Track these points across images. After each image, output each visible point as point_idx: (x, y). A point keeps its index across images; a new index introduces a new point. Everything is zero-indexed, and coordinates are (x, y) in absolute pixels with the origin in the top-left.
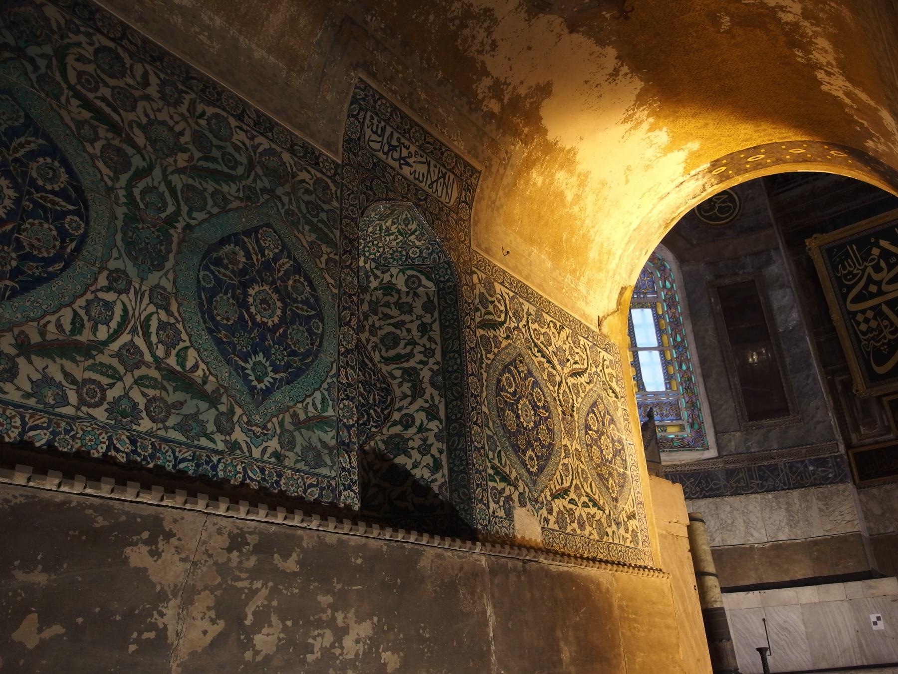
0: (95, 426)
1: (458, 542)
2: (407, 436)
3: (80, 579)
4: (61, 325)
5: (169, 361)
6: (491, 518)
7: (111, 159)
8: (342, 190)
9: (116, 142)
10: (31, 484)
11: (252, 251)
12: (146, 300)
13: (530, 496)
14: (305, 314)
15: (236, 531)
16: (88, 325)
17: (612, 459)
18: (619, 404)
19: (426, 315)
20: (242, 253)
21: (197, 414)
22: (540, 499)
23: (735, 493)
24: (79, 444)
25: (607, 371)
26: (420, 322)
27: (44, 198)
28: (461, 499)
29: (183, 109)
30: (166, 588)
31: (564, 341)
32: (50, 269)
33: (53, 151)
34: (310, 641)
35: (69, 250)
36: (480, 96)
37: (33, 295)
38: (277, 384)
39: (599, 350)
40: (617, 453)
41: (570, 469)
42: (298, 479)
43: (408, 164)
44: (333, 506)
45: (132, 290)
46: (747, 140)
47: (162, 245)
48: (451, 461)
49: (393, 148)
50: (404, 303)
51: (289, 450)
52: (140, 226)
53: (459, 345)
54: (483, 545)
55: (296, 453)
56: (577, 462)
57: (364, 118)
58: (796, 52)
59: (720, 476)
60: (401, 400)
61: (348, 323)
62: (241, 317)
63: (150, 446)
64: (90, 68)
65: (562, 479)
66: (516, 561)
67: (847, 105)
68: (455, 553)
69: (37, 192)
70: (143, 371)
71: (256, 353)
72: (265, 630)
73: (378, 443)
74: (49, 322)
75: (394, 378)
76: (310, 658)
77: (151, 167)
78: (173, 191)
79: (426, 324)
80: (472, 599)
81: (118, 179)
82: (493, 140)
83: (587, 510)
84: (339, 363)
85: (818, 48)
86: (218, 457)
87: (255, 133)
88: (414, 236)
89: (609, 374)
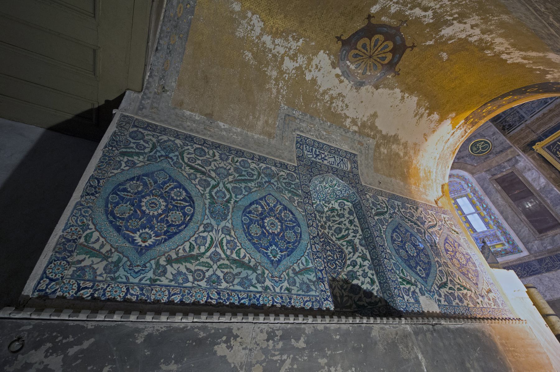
1: (391, 319)
2: (355, 271)
3: (193, 365)
4: (185, 249)
7: (203, 184)
8: (299, 175)
9: (204, 178)
10: (168, 321)
12: (220, 233)
14: (292, 225)
15: (270, 330)
16: (196, 247)
17: (466, 264)
18: (460, 237)
20: (260, 207)
21: (247, 277)
22: (432, 290)
24: (194, 299)
25: (448, 223)
28: (388, 296)
29: (230, 161)
30: (237, 365)
33: (180, 186)
35: (187, 220)
36: (348, 126)
37: (173, 240)
39: (440, 214)
40: (468, 260)
42: (300, 299)
43: (325, 160)
44: (320, 309)
45: (214, 230)
46: (478, 103)
49: (318, 155)
51: (294, 286)
54: (406, 319)
56: (447, 269)
58: (487, 52)
62: (263, 232)
65: (441, 278)
66: (428, 326)
67: (526, 64)
68: (391, 325)
70: (222, 262)
71: (271, 245)
73: (343, 276)
75: (344, 246)
77: (218, 184)
78: (228, 190)
80: (408, 350)
81: (206, 190)
83: (461, 292)
85: (497, 44)
86: (259, 295)
88: (336, 186)
89: (449, 224)
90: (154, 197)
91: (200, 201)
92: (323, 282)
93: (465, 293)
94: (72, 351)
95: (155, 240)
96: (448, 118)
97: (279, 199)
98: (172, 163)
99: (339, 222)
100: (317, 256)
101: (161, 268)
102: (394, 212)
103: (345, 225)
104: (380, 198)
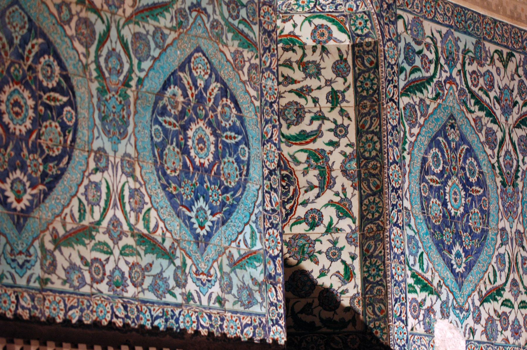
0: (103, 299)
2: (313, 237)
6: (410, 336)
7: (83, 34)
9: (83, 14)
11: (187, 86)
13: (455, 303)
14: (233, 141)
16: (88, 209)
20: (180, 92)
21: (161, 273)
26: (329, 89)
27: (49, 98)
31: (512, 76)
32: (61, 165)
35: (69, 142)
38: (215, 226)
41: (507, 260)
45: (110, 166)
47: (123, 110)
48: (365, 270)
50: (309, 62)
52: (108, 97)
53: (380, 125)
55: (234, 295)
56: (517, 249)
60: (306, 191)
61: (270, 140)
62: (185, 165)
63: (136, 309)
65: (495, 275)
69: (45, 94)
71: (197, 199)
74: (66, 214)
75: (298, 163)
77: (109, 28)
79: (338, 91)
84: (264, 188)
86: (179, 310)
91: (84, 89)
92: (274, 285)
95: (32, 195)
99: (302, 89)
100: (272, 224)
101: (48, 257)
102: (450, 80)
103: (315, 101)
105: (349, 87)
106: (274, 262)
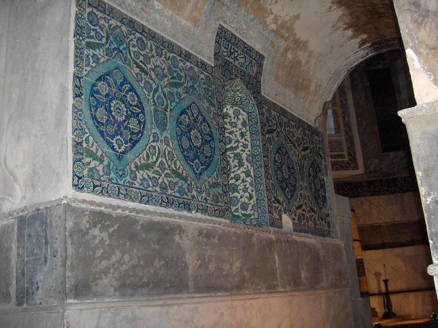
5: (172, 166)
8: (215, 79)
9: (147, 79)
11: (190, 115)
12: (164, 144)
14: (208, 139)
16: (150, 156)
19: (243, 128)
20: (187, 117)
21: (182, 186)
22: (292, 210)
23: (373, 195)
25: (318, 146)
26: (240, 132)
27: (133, 109)
34: (224, 267)
39: (314, 135)
43: (237, 60)
49: (232, 53)
52: (158, 113)
55: (211, 198)
57: (221, 42)
59: (364, 185)
60: (234, 168)
64: (136, 49)
65: (300, 200)
71: (196, 159)
72: (211, 263)
75: (231, 158)
76: (224, 273)
77: (158, 87)
78: (165, 95)
82: (272, 41)
83: (310, 214)
87: (185, 61)
88: (238, 92)
89: (318, 147)
90: (118, 101)
92: (226, 196)
93: (312, 215)
94: (111, 230)
96: (359, 38)
97: (201, 109)
98: (123, 59)
100: (224, 172)
103: (236, 136)
104: (273, 112)
105: (247, 131)
106: (226, 187)
